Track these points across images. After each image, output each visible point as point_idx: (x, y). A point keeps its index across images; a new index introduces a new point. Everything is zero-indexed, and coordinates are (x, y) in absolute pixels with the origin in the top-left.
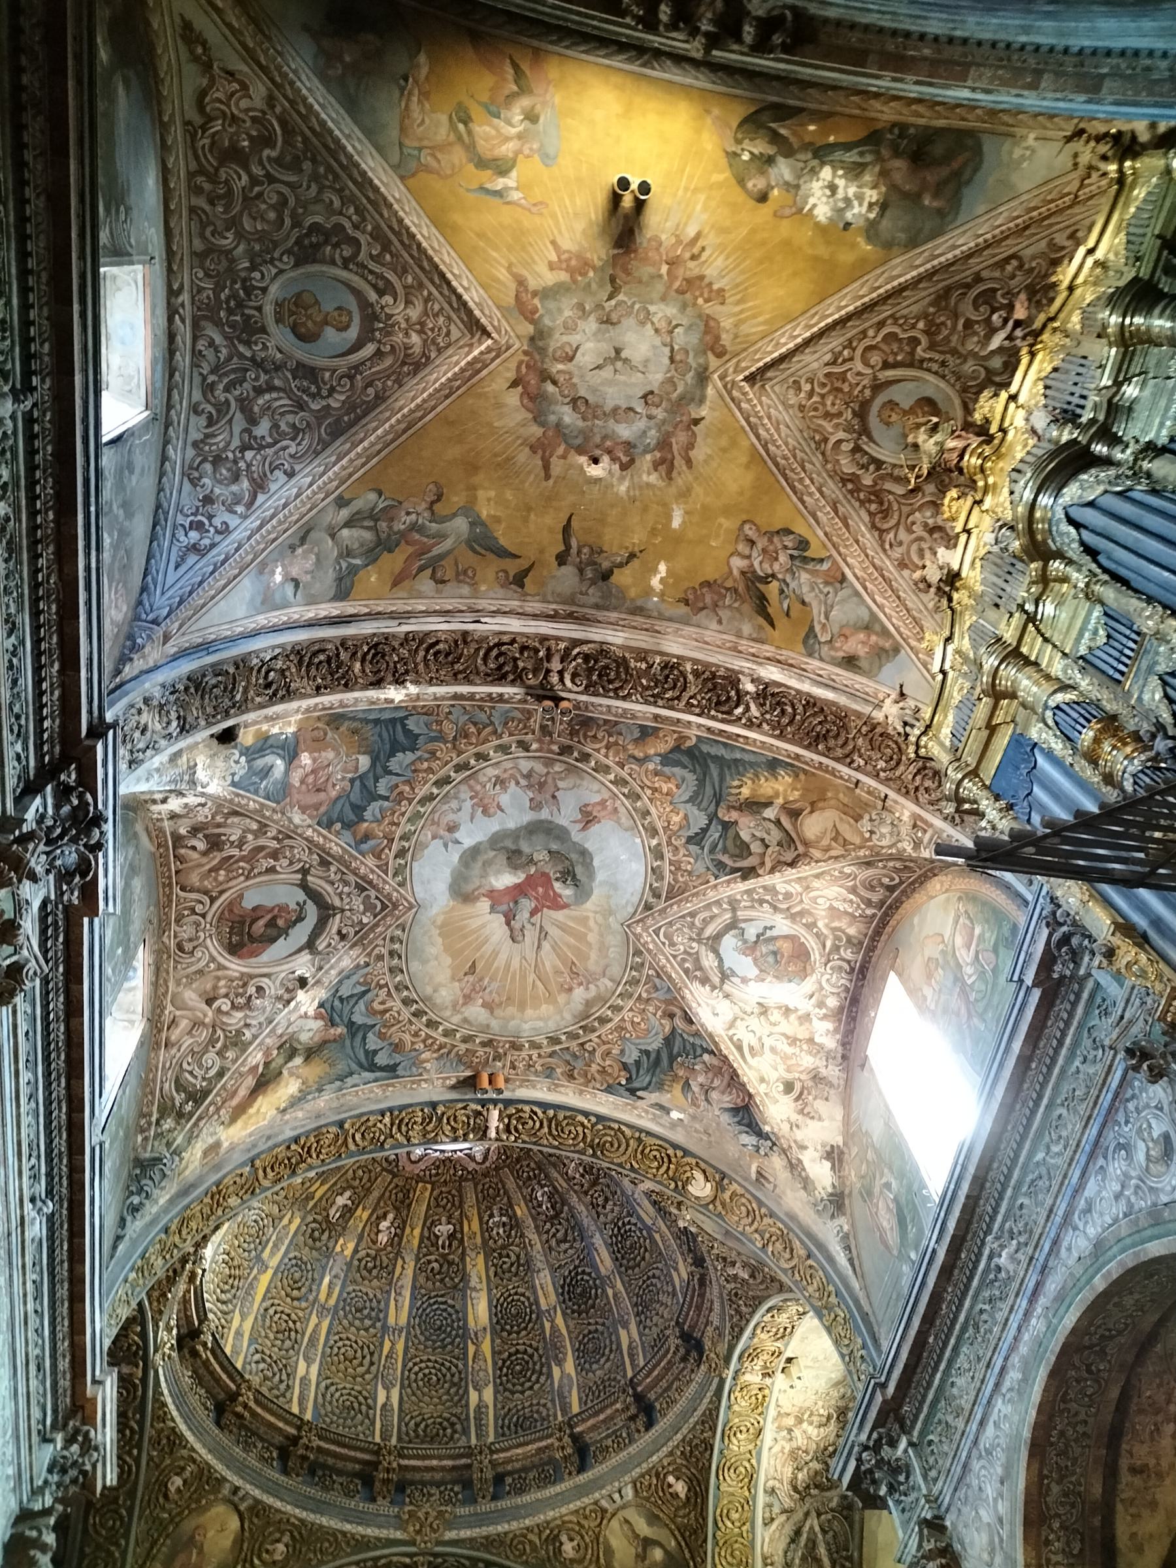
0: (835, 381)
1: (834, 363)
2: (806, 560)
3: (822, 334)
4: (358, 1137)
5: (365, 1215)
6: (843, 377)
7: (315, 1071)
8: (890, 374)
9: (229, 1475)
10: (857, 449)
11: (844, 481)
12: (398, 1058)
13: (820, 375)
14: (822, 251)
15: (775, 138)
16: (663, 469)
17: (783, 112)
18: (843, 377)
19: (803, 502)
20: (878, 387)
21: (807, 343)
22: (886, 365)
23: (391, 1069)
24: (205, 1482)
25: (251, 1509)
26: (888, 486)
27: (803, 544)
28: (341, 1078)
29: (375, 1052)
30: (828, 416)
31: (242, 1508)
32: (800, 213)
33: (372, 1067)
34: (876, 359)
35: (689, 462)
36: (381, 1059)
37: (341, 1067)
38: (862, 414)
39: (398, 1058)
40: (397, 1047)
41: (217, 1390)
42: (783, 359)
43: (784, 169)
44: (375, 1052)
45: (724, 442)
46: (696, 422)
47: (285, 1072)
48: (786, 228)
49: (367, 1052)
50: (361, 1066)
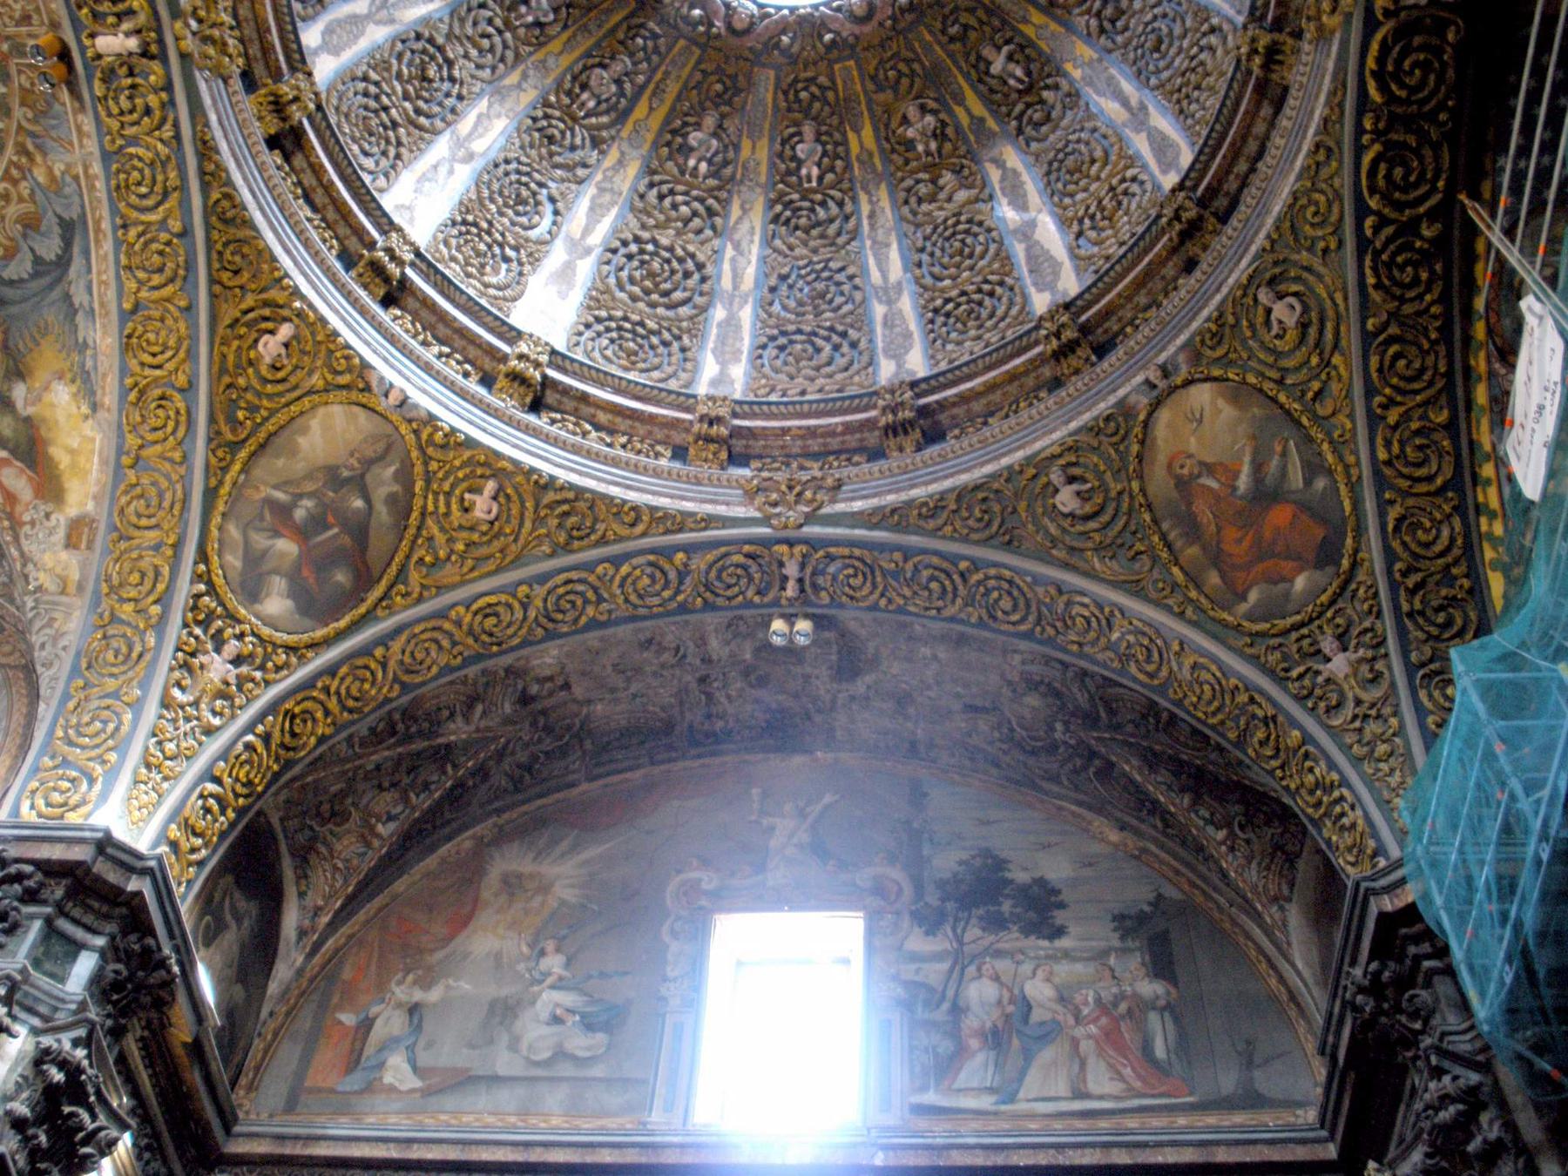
4: (157, 279)
5: (1037, 17)
7: (47, 359)
9: (1121, 393)
12: (50, 221)
23: (70, 229)
24: (1124, 431)
25: (1196, 357)
28: (72, 311)
29: (38, 260)
31: (1183, 372)
33: (63, 262)
36: (50, 248)
37: (52, 315)
39: (50, 221)
40: (30, 224)
41: (1030, 381)
44: (38, 260)
47: (30, 411)
49: (36, 275)
50: (59, 280)
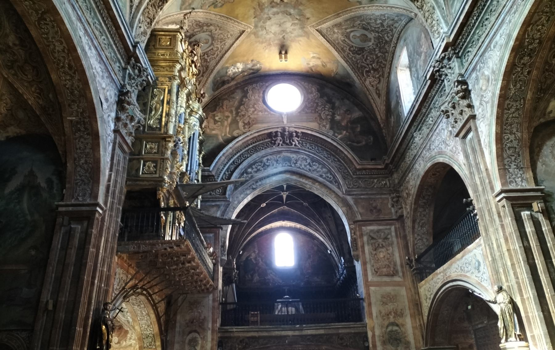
0: (222, 40)
1: (224, 44)
2: (213, 4)
3: (230, 47)
6: (221, 42)
8: (210, 48)
10: (211, 31)
11: (211, 25)
13: (227, 40)
14: (236, 59)
15: (253, 70)
16: (261, 4)
17: (253, 73)
18: (221, 42)
19: (220, 15)
20: (212, 44)
21: (233, 44)
22: (212, 49)
26: (199, 29)
27: (215, 6)
30: (222, 34)
32: (243, 62)
34: (215, 49)
35: (254, 8)
38: (213, 39)
42: (237, 39)
43: (249, 66)
45: (246, 16)
46: (255, 17)
48: (245, 58)
